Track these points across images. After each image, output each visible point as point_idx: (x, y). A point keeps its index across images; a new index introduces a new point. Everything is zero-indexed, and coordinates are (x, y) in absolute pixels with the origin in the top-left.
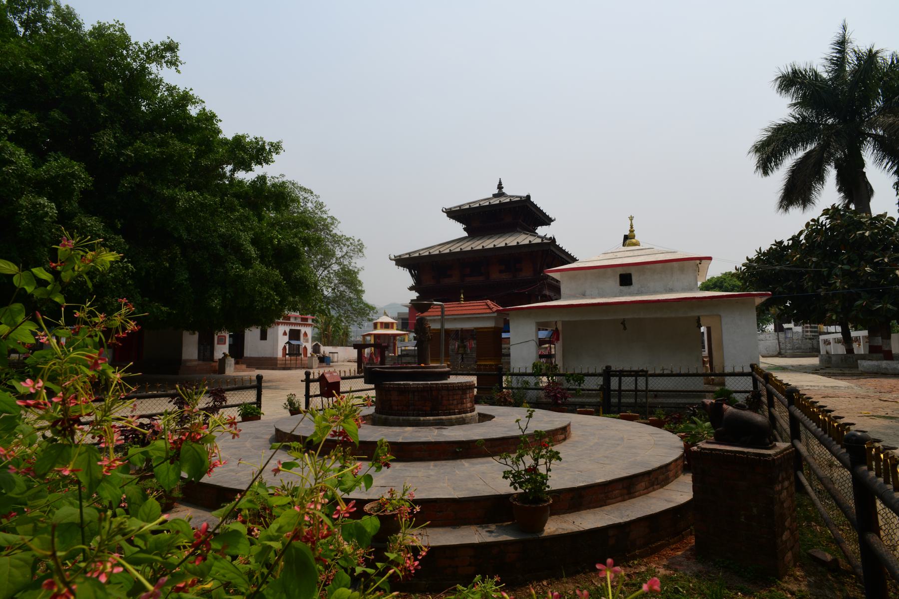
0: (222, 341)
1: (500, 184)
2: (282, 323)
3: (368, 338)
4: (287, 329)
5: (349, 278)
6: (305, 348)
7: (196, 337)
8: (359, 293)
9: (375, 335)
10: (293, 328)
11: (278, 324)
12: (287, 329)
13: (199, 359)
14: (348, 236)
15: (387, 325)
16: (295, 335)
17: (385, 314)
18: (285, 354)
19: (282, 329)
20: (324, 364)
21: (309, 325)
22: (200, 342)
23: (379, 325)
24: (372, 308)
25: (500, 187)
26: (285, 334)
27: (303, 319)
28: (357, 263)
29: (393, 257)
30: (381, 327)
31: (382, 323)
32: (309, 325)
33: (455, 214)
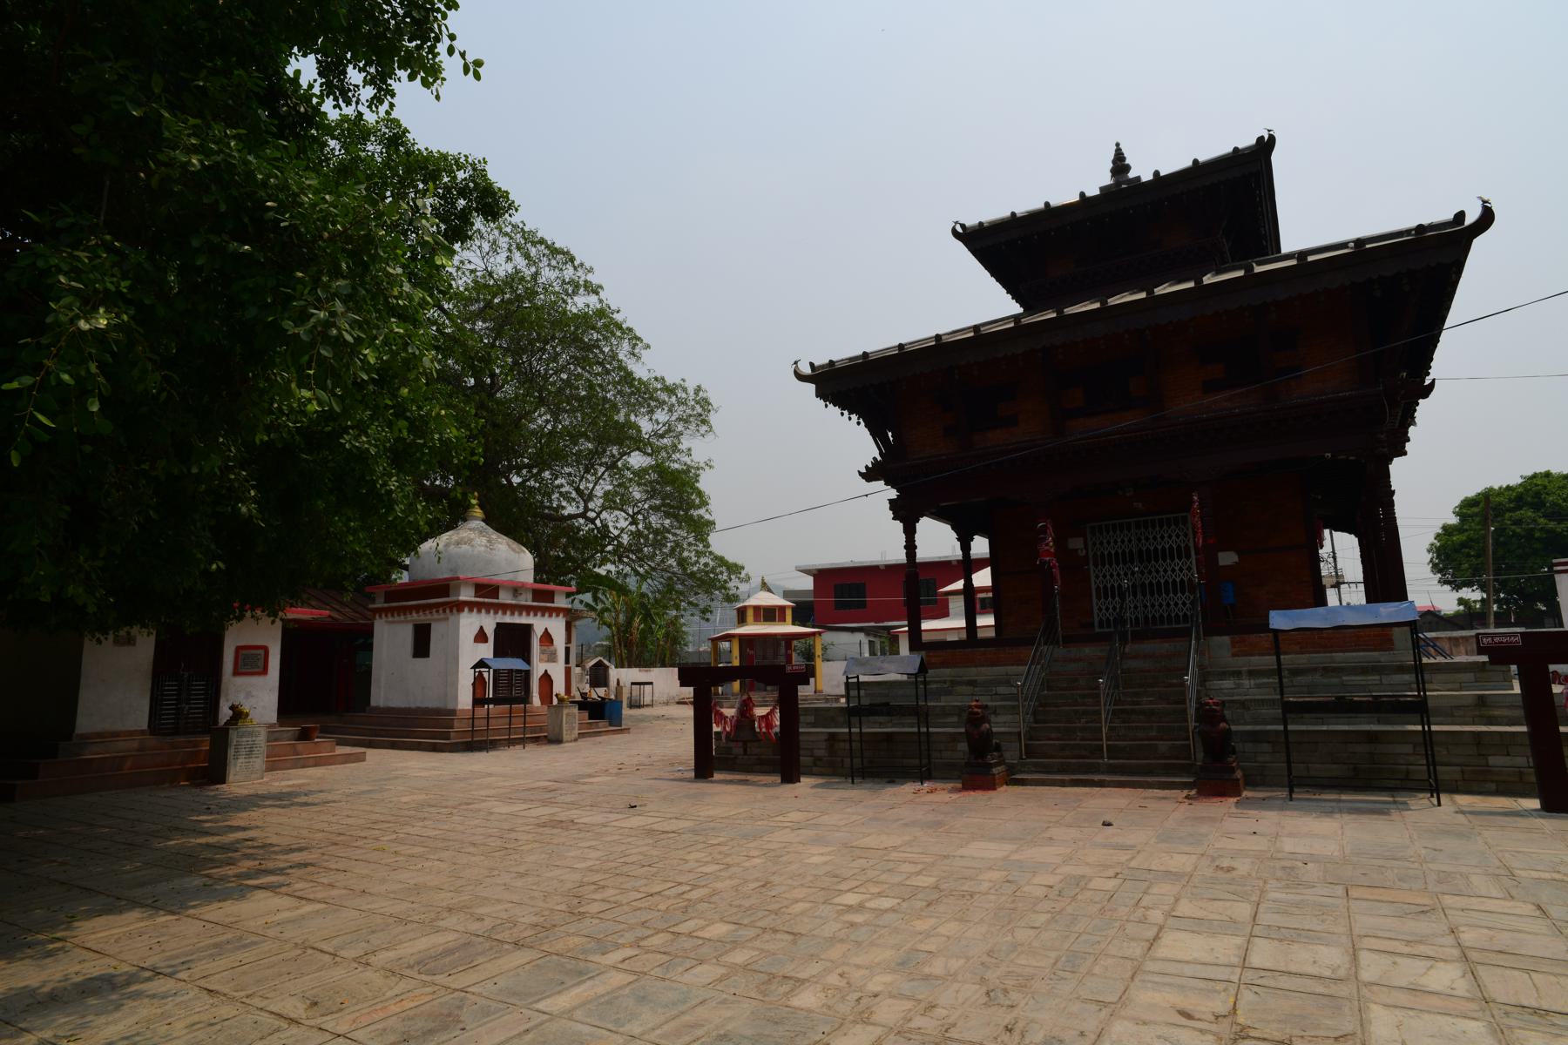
0: (251, 662)
1: (1119, 158)
2: (471, 606)
3: (725, 645)
4: (489, 622)
5: (677, 493)
6: (546, 679)
7: (144, 648)
8: (701, 528)
9: (742, 637)
10: (508, 619)
11: (460, 606)
12: (489, 622)
13: (155, 726)
14: (669, 381)
15: (769, 614)
16: (513, 641)
17: (765, 587)
18: (478, 701)
19: (469, 623)
20: (603, 725)
21: (558, 611)
22: (163, 669)
23: (750, 613)
24: (735, 569)
25: (1120, 165)
26: (481, 637)
27: (538, 595)
28: (695, 448)
29: (807, 370)
30: (757, 619)
31: (757, 608)
32: (558, 611)
33: (995, 245)
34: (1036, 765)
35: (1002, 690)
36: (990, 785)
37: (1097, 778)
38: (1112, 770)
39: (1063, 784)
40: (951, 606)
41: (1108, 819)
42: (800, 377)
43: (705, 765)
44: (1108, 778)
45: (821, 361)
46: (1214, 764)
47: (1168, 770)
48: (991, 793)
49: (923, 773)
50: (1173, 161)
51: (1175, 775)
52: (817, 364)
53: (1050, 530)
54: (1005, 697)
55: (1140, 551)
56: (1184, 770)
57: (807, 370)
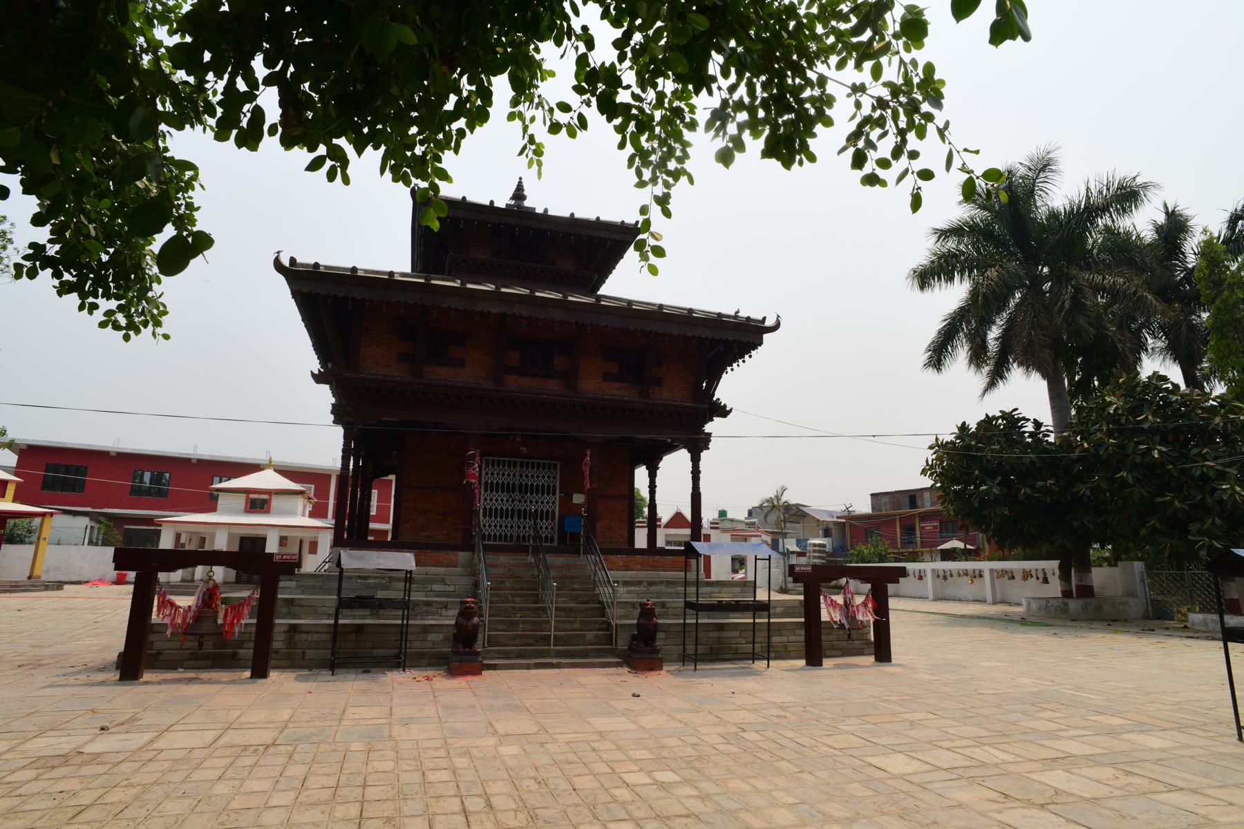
1: (520, 188)
25: (519, 194)
29: (286, 263)
34: (498, 652)
35: (436, 587)
36: (477, 672)
37: (554, 661)
38: (559, 654)
39: (528, 667)
40: (220, 502)
41: (637, 692)
42: (278, 265)
43: (134, 662)
44: (554, 661)
45: (306, 258)
46: (641, 649)
47: (600, 653)
48: (474, 680)
49: (398, 661)
50: (559, 210)
51: (603, 657)
52: (299, 261)
53: (478, 459)
54: (439, 594)
55: (521, 485)
56: (612, 653)
57: (286, 263)
